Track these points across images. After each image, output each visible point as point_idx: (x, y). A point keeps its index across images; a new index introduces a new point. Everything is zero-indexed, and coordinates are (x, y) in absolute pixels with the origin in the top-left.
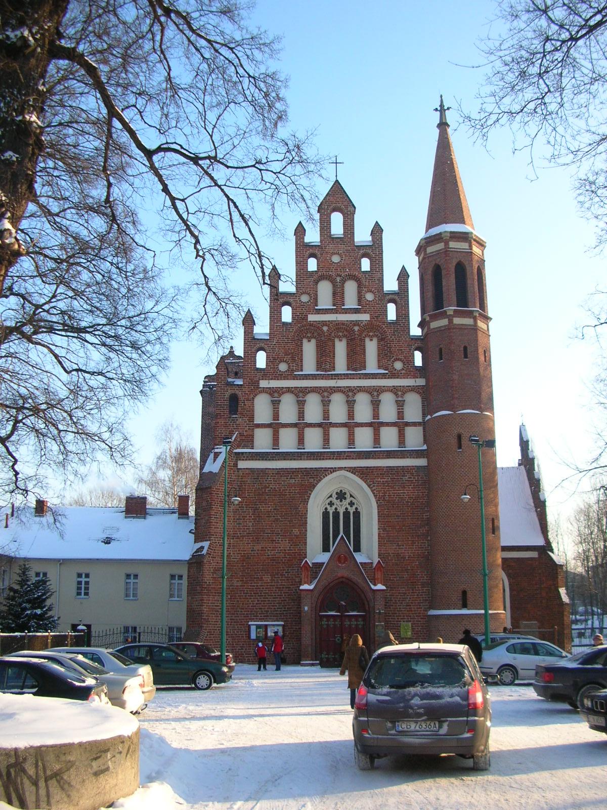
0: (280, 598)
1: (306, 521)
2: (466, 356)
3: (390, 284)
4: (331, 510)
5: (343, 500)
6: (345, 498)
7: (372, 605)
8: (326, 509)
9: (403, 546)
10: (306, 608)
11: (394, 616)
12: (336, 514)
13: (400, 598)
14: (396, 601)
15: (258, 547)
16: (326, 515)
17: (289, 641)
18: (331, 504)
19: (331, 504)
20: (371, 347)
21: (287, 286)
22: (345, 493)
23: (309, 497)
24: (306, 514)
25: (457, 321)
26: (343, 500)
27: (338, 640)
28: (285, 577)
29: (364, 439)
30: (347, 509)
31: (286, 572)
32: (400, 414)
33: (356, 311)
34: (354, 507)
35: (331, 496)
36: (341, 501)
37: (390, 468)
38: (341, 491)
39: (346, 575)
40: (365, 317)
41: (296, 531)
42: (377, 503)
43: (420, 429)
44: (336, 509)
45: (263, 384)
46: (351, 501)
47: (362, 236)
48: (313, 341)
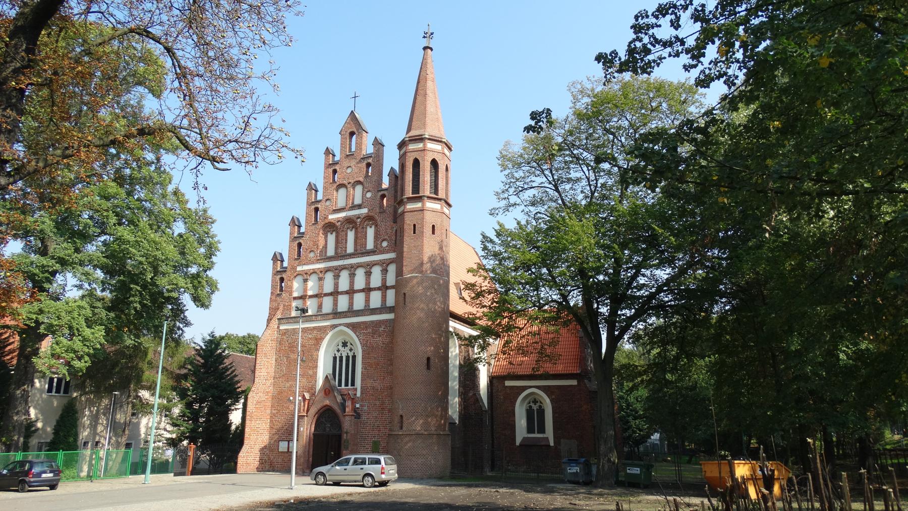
2: (414, 233)
3: (386, 183)
4: (338, 355)
12: (341, 358)
15: (288, 385)
16: (335, 358)
18: (338, 351)
19: (338, 351)
20: (371, 232)
21: (320, 196)
25: (410, 206)
29: (359, 301)
32: (384, 280)
33: (359, 207)
37: (372, 322)
40: (364, 211)
41: (311, 372)
43: (394, 291)
45: (299, 269)
47: (369, 149)
48: (334, 234)
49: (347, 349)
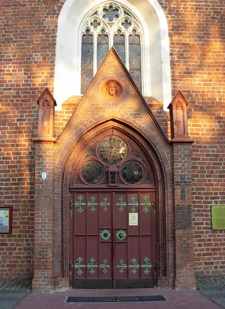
0: (7, 163)
1: (55, 40)
4: (96, 32)
5: (114, 19)
6: (117, 16)
7: (168, 169)
8: (88, 30)
9: (211, 81)
10: (44, 176)
11: (199, 194)
13: (210, 164)
14: (202, 168)
17: (20, 236)
18: (96, 23)
22: (117, 10)
23: (61, 7)
24: (54, 31)
26: (114, 19)
27: (105, 235)
28: (17, 128)
30: (119, 30)
31: (18, 120)
34: (131, 28)
35: (96, 13)
36: (111, 20)
38: (111, 7)
39: (118, 117)
42: (167, 17)
44: (103, 30)
46: (126, 21)
49: (117, 24)
